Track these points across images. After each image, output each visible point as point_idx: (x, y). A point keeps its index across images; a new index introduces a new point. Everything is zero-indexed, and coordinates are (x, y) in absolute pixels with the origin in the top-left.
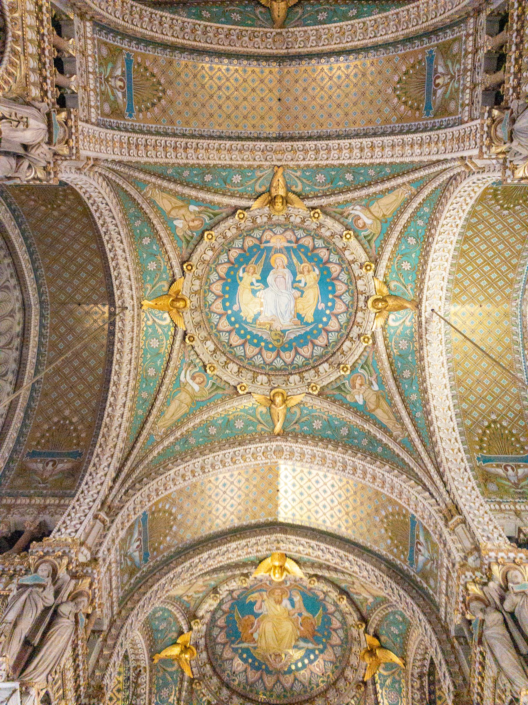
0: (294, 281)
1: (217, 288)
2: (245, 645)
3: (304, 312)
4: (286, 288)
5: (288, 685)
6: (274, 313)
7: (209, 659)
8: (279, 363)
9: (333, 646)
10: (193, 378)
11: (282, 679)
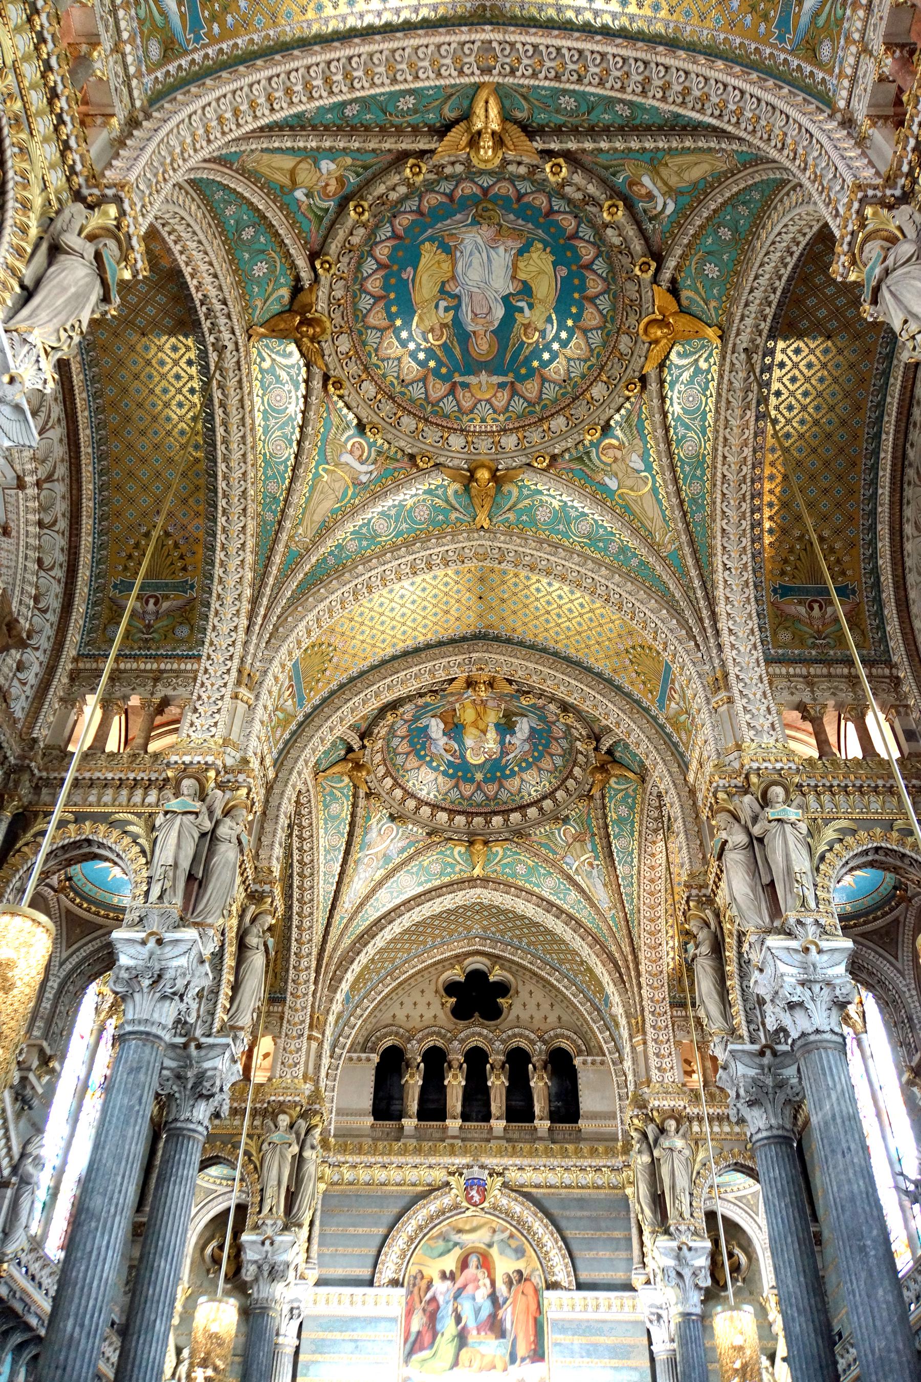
8: (479, 797)
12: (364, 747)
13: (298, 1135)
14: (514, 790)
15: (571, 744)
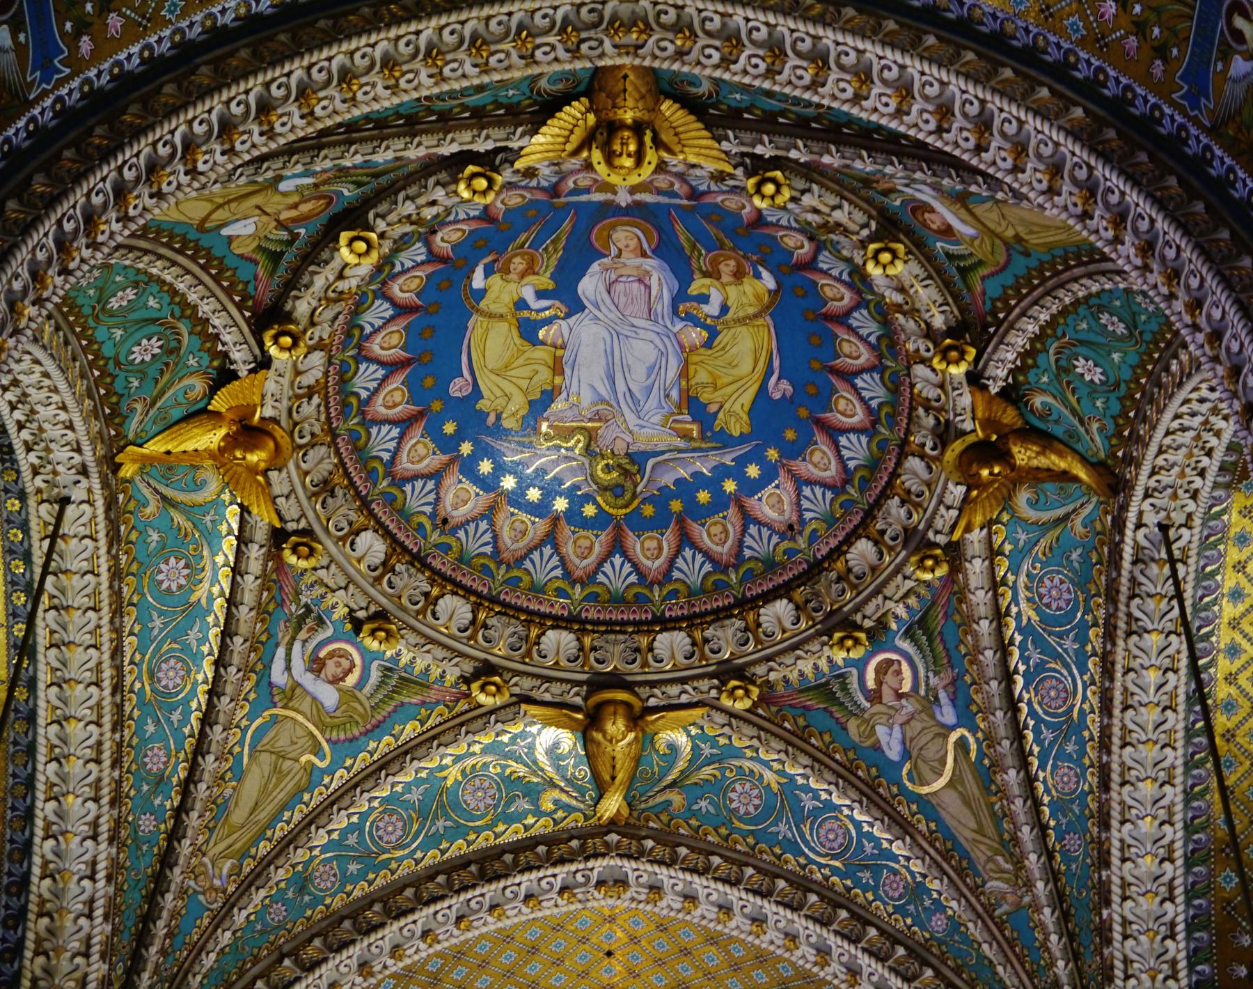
0: (679, 298)
3: (718, 396)
4: (650, 314)
6: (604, 392)
8: (617, 576)
10: (316, 665)
12: (264, 363)
15: (897, 385)
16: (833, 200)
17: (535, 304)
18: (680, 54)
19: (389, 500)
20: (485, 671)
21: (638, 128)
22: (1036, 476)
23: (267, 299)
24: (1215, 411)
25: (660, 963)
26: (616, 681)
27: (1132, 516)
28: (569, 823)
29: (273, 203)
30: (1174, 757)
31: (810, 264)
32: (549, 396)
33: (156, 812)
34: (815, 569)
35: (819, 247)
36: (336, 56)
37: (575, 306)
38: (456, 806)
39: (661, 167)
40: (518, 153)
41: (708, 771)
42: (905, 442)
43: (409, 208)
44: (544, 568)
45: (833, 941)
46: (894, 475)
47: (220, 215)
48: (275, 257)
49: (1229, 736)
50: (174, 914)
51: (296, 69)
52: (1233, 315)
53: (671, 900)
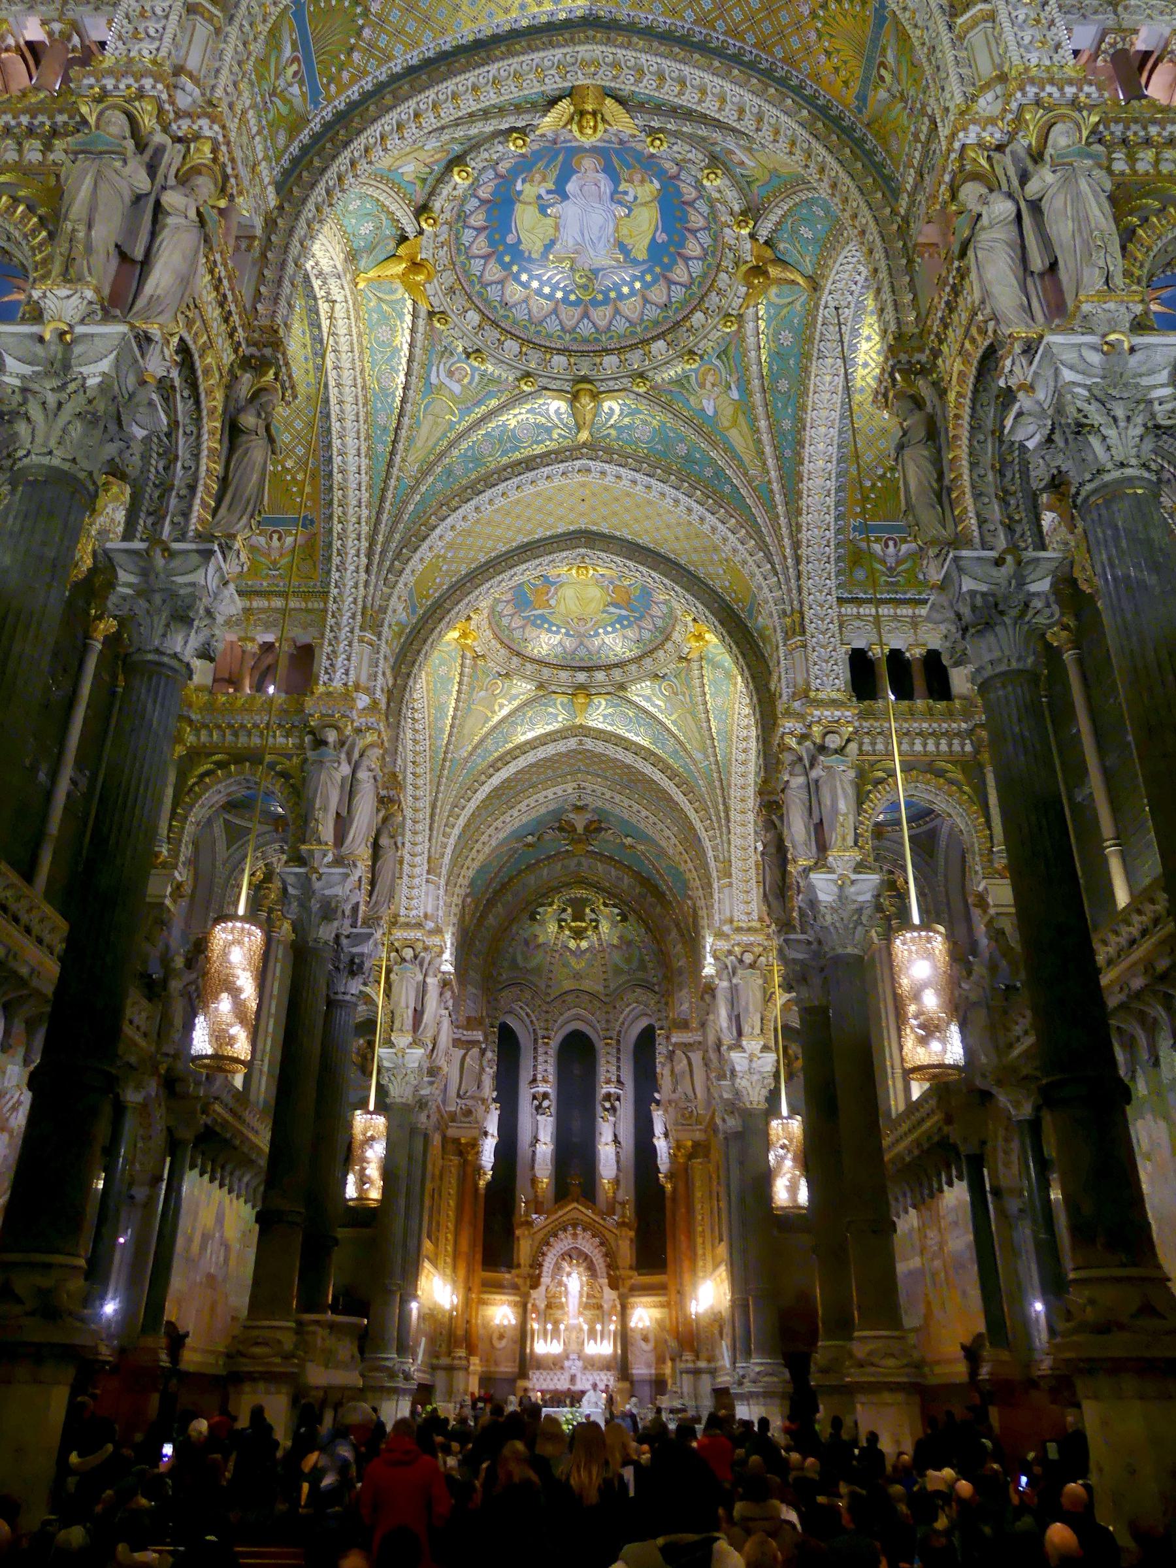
0: (615, 192)
1: (478, 220)
2: (539, 612)
5: (593, 649)
7: (495, 634)
8: (586, 329)
9: (652, 616)
10: (450, 374)
11: (585, 640)
12: (421, 232)
13: (349, 755)
14: (634, 316)
15: (716, 237)
16: (688, 148)
17: (546, 197)
18: (615, 78)
19: (480, 294)
20: (528, 375)
21: (594, 114)
22: (780, 281)
23: (421, 202)
24: (859, 262)
25: (605, 504)
26: (585, 379)
27: (823, 303)
28: (565, 444)
29: (422, 155)
30: (835, 415)
31: (677, 177)
32: (553, 242)
33: (384, 443)
34: (677, 324)
35: (681, 169)
36: (450, 85)
37: (565, 196)
38: (514, 436)
39: (606, 131)
40: (537, 127)
41: (627, 420)
42: (719, 265)
43: (486, 155)
44: (552, 326)
45: (681, 496)
46: (714, 280)
47: (398, 163)
48: (424, 180)
49: (860, 404)
50: (396, 488)
51: (431, 93)
52: (872, 223)
53: (610, 478)
